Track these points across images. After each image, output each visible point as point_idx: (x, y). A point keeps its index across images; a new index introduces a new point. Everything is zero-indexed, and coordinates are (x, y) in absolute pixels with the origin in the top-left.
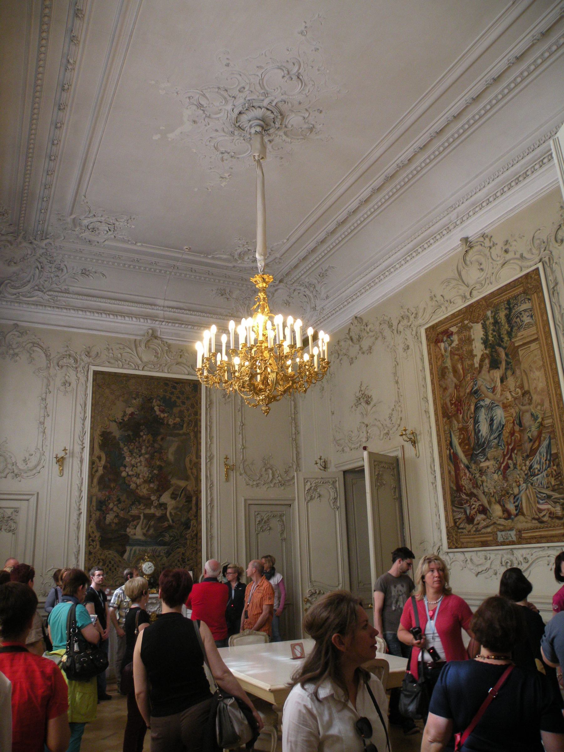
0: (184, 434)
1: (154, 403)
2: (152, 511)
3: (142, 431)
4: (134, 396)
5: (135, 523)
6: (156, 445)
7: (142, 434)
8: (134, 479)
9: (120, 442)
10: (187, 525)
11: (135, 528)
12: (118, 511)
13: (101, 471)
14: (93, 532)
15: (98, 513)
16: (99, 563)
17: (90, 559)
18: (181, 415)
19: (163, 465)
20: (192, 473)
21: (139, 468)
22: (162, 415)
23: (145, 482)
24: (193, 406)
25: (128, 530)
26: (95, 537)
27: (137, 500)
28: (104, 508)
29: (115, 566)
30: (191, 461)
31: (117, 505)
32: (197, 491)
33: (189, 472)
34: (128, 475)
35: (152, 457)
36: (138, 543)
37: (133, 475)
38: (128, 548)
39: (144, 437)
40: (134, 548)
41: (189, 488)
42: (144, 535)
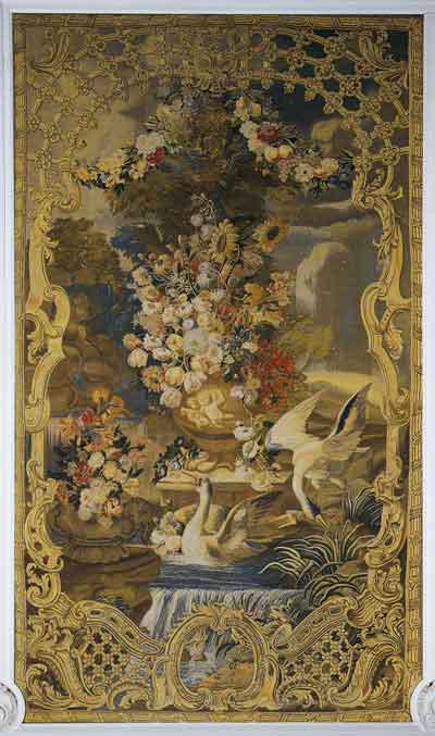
0: (356, 214)
1: (241, 110)
2: (240, 475)
3: (195, 211)
4: (164, 92)
5: (180, 514)
6: (249, 257)
7: (196, 220)
8: (174, 373)
9: (121, 253)
10: (367, 519)
11: (181, 533)
12: (122, 478)
13: (56, 351)
14: (38, 545)
15: (53, 485)
16: (61, 638)
17: (30, 628)
18: (343, 147)
19: (276, 323)
20: (385, 345)
21: (190, 336)
22: (270, 153)
23: (211, 380)
24: (388, 112)
25: (156, 537)
26: (46, 560)
27: (186, 442)
28: (72, 468)
29: (115, 649)
30: (380, 307)
31: (115, 458)
32: (406, 406)
33: (374, 343)
34: (151, 361)
35: (237, 296)
36: (194, 577)
37: (170, 361)
38: (157, 595)
39: (205, 229)
40: (178, 594)
41: (373, 396)
42: (213, 553)
